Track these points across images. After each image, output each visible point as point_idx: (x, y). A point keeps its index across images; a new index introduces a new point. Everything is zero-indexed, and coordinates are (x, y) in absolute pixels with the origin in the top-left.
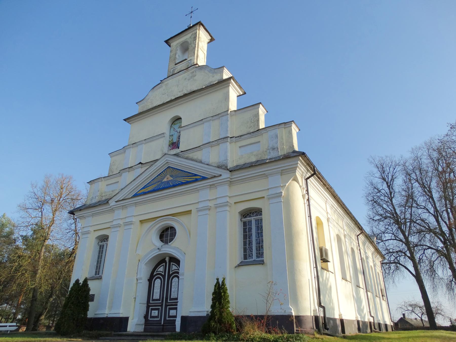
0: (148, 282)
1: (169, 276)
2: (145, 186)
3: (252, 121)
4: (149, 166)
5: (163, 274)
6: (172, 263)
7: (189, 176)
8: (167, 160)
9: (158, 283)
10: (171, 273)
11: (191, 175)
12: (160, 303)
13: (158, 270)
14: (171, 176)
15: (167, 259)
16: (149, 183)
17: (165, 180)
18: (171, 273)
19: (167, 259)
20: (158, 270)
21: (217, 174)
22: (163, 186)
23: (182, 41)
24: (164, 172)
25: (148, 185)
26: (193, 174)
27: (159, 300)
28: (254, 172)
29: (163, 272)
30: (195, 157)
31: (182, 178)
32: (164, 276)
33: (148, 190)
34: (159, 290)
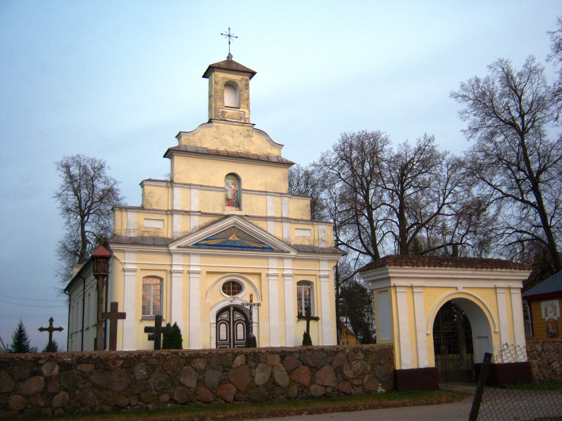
0: (49, 322)
1: (234, 322)
2: (208, 238)
3: (305, 210)
4: (256, 222)
5: (228, 320)
6: (235, 312)
7: (256, 243)
8: (235, 220)
9: (223, 327)
10: (235, 320)
11: (257, 241)
12: (228, 343)
13: (222, 317)
14: (238, 237)
15: (232, 309)
16: (213, 236)
17: (231, 238)
18: (235, 320)
19: (232, 309)
20: (222, 317)
21: (286, 250)
22: (230, 243)
23: (230, 79)
24: (239, 231)
25: (212, 238)
26: (260, 241)
27: (226, 340)
28: (308, 256)
29: (227, 318)
30: (260, 226)
31: (257, 244)
32: (229, 322)
33: (212, 243)
34: (225, 333)
